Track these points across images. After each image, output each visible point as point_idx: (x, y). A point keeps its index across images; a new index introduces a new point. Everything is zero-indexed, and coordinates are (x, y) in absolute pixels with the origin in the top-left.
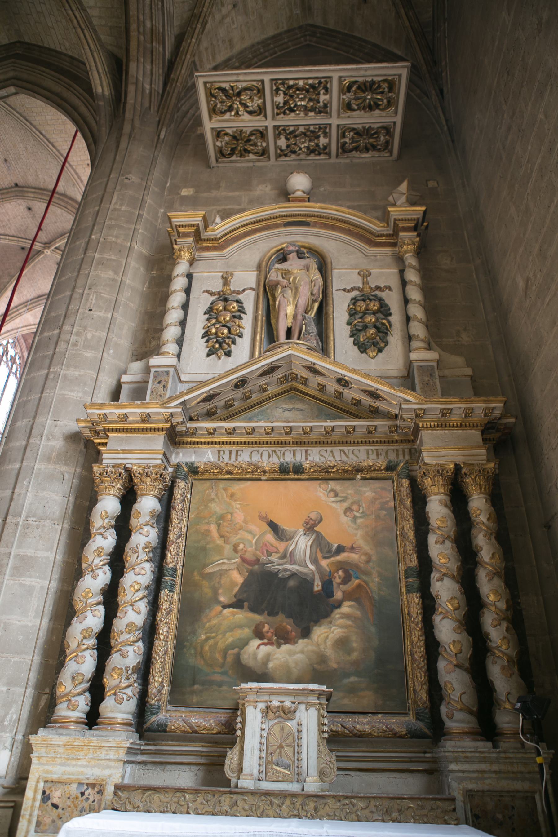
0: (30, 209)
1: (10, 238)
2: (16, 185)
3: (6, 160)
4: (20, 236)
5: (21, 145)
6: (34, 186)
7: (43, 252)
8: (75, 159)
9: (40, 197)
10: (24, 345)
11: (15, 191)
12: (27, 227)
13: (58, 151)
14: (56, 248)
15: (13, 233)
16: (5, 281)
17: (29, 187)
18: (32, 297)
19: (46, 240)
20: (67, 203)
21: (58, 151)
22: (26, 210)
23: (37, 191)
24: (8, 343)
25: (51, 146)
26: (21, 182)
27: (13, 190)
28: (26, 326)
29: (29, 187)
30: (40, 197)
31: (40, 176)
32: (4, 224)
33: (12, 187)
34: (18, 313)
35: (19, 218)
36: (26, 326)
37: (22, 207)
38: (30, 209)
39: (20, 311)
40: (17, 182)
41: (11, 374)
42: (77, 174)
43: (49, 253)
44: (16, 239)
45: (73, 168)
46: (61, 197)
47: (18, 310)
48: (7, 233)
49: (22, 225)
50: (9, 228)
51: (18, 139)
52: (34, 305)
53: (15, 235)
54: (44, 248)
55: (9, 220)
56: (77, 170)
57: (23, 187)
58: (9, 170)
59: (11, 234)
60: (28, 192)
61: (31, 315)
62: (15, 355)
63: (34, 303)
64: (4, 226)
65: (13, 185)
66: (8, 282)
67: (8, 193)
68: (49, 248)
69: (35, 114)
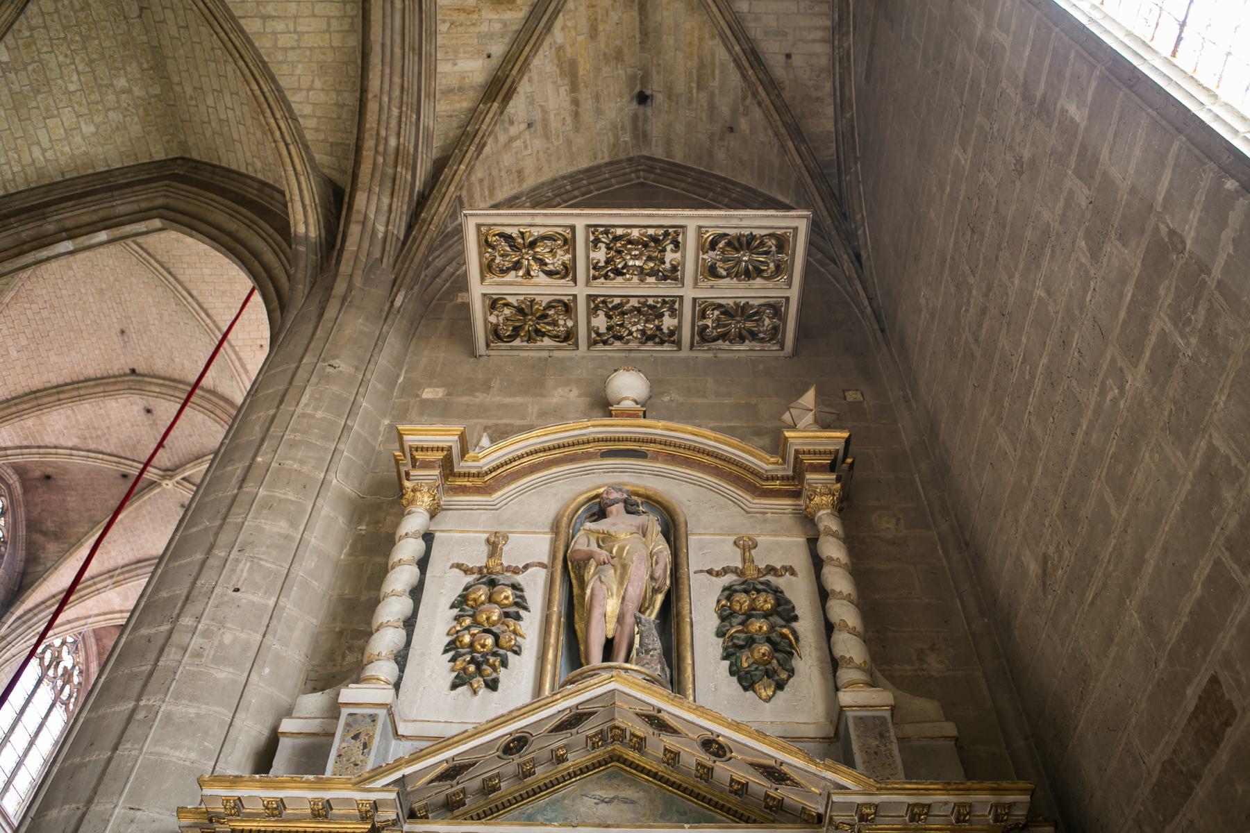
0: (149, 411)
1: (106, 457)
2: (133, 371)
3: (123, 332)
5: (154, 310)
6: (163, 374)
7: (160, 485)
8: (240, 336)
9: (171, 392)
10: (95, 648)
12: (139, 441)
13: (214, 322)
14: (183, 479)
15: (111, 448)
16: (82, 530)
17: (154, 376)
18: (126, 561)
19: (169, 465)
20: (216, 405)
21: (214, 322)
22: (143, 413)
23: (167, 383)
24: (64, 643)
25: (203, 315)
26: (141, 367)
28: (105, 614)
29: (154, 376)
30: (171, 392)
31: (177, 360)
32: (99, 433)
33: (125, 375)
34: (93, 588)
35: (128, 424)
36: (105, 614)
37: (135, 408)
38: (149, 411)
39: (99, 586)
41: (58, 704)
42: (240, 359)
43: (170, 486)
44: (115, 459)
45: (235, 351)
46: (207, 395)
47: (95, 584)
48: (101, 448)
49: (130, 438)
50: (107, 441)
51: (150, 300)
52: (127, 575)
53: (115, 452)
54: (163, 477)
55: (108, 428)
56: (241, 354)
57: (144, 375)
58: (125, 347)
59: (108, 451)
60: (150, 383)
61: (119, 593)
62: (74, 667)
63: (128, 572)
64: (98, 437)
66: (87, 533)
67: (115, 383)
68: (171, 477)
69: (185, 266)
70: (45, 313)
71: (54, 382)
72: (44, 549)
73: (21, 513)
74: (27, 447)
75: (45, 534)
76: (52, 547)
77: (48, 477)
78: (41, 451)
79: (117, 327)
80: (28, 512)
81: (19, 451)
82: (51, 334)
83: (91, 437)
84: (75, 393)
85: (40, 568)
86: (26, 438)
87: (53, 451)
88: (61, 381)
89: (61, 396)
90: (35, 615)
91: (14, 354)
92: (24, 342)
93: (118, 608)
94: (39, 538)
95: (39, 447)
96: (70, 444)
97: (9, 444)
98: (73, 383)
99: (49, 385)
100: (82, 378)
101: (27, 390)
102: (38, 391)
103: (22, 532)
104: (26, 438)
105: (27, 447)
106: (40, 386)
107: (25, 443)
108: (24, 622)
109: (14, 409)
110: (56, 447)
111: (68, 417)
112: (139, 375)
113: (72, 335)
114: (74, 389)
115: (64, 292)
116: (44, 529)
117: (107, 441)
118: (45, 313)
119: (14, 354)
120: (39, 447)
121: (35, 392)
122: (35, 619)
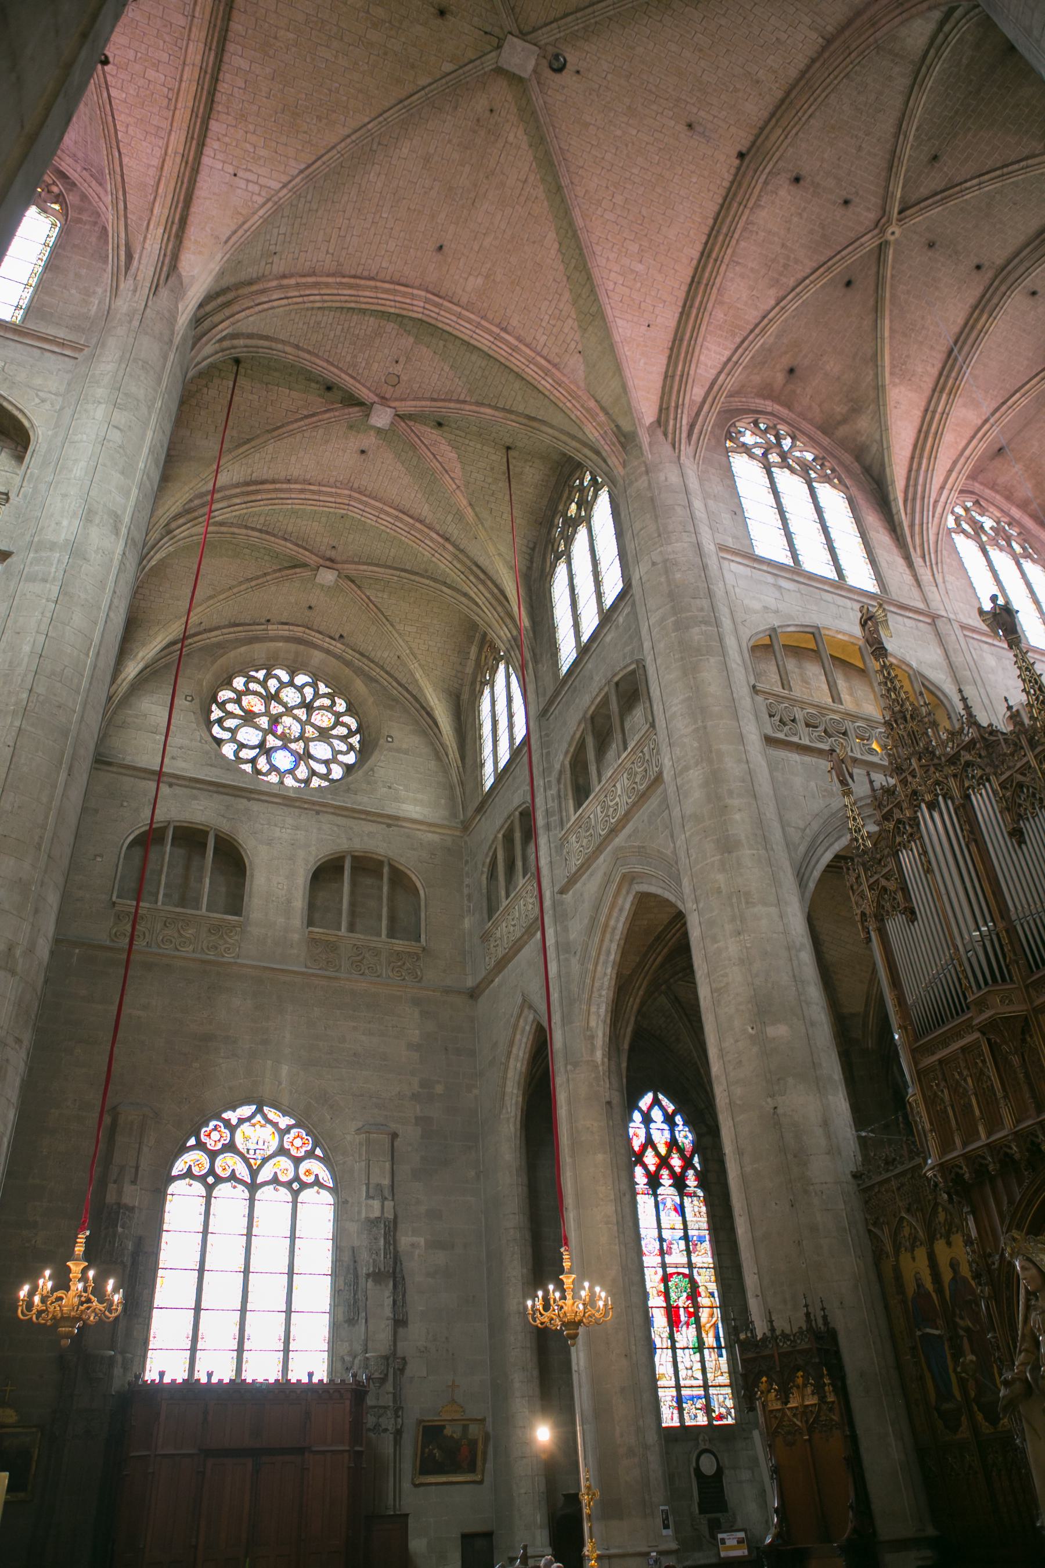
0: (797, 180)
1: (812, 278)
2: (741, 155)
3: (690, 126)
4: (823, 259)
6: (765, 114)
7: (887, 243)
10: (998, 497)
11: (748, 167)
14: (900, 212)
16: (869, 378)
18: (939, 365)
19: (872, 216)
24: (967, 510)
27: (743, 169)
28: (973, 437)
32: (782, 261)
33: (738, 169)
34: (937, 417)
35: (795, 219)
36: (973, 437)
37: (782, 193)
38: (797, 180)
39: (940, 409)
40: (739, 148)
41: (1022, 561)
44: (822, 270)
47: (934, 412)
48: (800, 276)
50: (797, 261)
52: (954, 374)
53: (815, 265)
54: (883, 231)
59: (808, 271)
60: (767, 137)
61: (965, 405)
62: (998, 523)
64: (785, 266)
65: (738, 162)
66: (876, 375)
67: (740, 185)
68: (889, 221)
70: (619, 199)
71: (696, 255)
72: (858, 432)
73: (805, 426)
74: (743, 342)
75: (844, 420)
76: (864, 423)
77: (791, 371)
78: (757, 331)
79: (681, 127)
80: (811, 421)
81: (740, 351)
82: (644, 212)
83: (781, 274)
84: (721, 238)
85: (874, 448)
86: (734, 335)
87: (766, 321)
88: (699, 247)
89: (714, 256)
90: (916, 485)
91: (640, 268)
92: (634, 248)
93: (980, 422)
94: (842, 431)
95: (752, 331)
96: (772, 302)
97: (727, 353)
98: (709, 236)
99: (695, 262)
100: (710, 222)
101: (685, 288)
102: (693, 277)
103: (826, 441)
104: (734, 335)
105: (743, 342)
106: (690, 272)
107: (738, 340)
108: (914, 499)
109: (694, 312)
110: (764, 317)
111: (742, 276)
112: (749, 150)
113: (659, 190)
114: (716, 237)
115: (609, 156)
116: (839, 418)
117: (797, 261)
118: (619, 199)
119: (640, 268)
120: (752, 331)
121: (692, 281)
122: (920, 488)
